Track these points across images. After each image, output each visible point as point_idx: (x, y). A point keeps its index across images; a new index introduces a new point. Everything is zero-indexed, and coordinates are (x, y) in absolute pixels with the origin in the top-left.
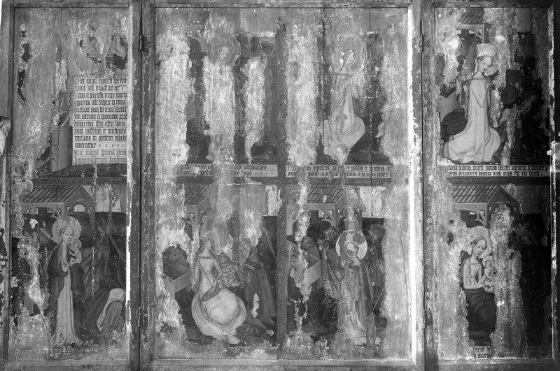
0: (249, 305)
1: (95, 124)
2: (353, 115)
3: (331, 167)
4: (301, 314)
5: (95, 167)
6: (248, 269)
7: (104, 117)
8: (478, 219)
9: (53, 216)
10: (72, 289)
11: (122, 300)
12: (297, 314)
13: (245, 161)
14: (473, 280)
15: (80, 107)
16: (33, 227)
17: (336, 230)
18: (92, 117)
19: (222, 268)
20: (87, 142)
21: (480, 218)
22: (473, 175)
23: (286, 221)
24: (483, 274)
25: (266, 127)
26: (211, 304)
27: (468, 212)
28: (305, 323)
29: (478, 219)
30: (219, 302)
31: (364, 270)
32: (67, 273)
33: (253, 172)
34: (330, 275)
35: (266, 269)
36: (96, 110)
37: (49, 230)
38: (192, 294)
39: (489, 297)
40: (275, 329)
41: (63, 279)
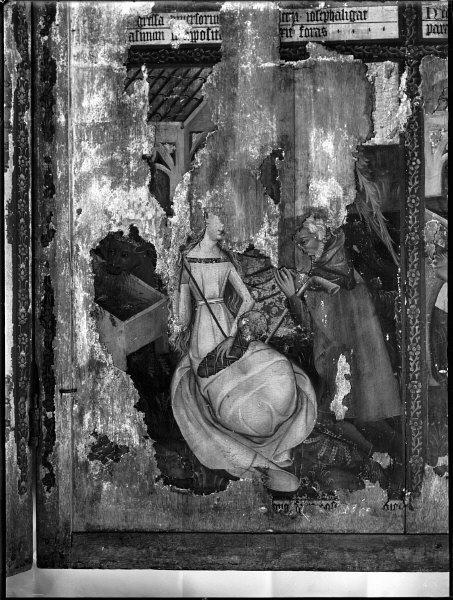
0: (324, 388)
6: (321, 289)
19: (251, 287)
23: (421, 157)
26: (223, 384)
30: (243, 378)
35: (371, 287)
38: (172, 359)
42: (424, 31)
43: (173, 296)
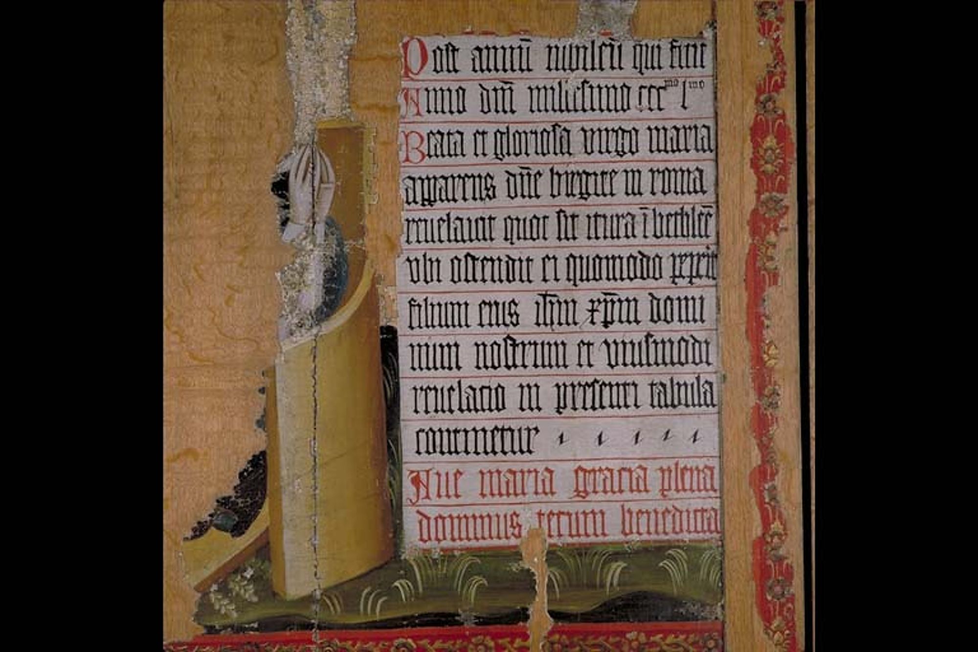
1: (527, 311)
5: (535, 562)
7: (582, 269)
18: (513, 270)
20: (486, 420)
36: (532, 229)
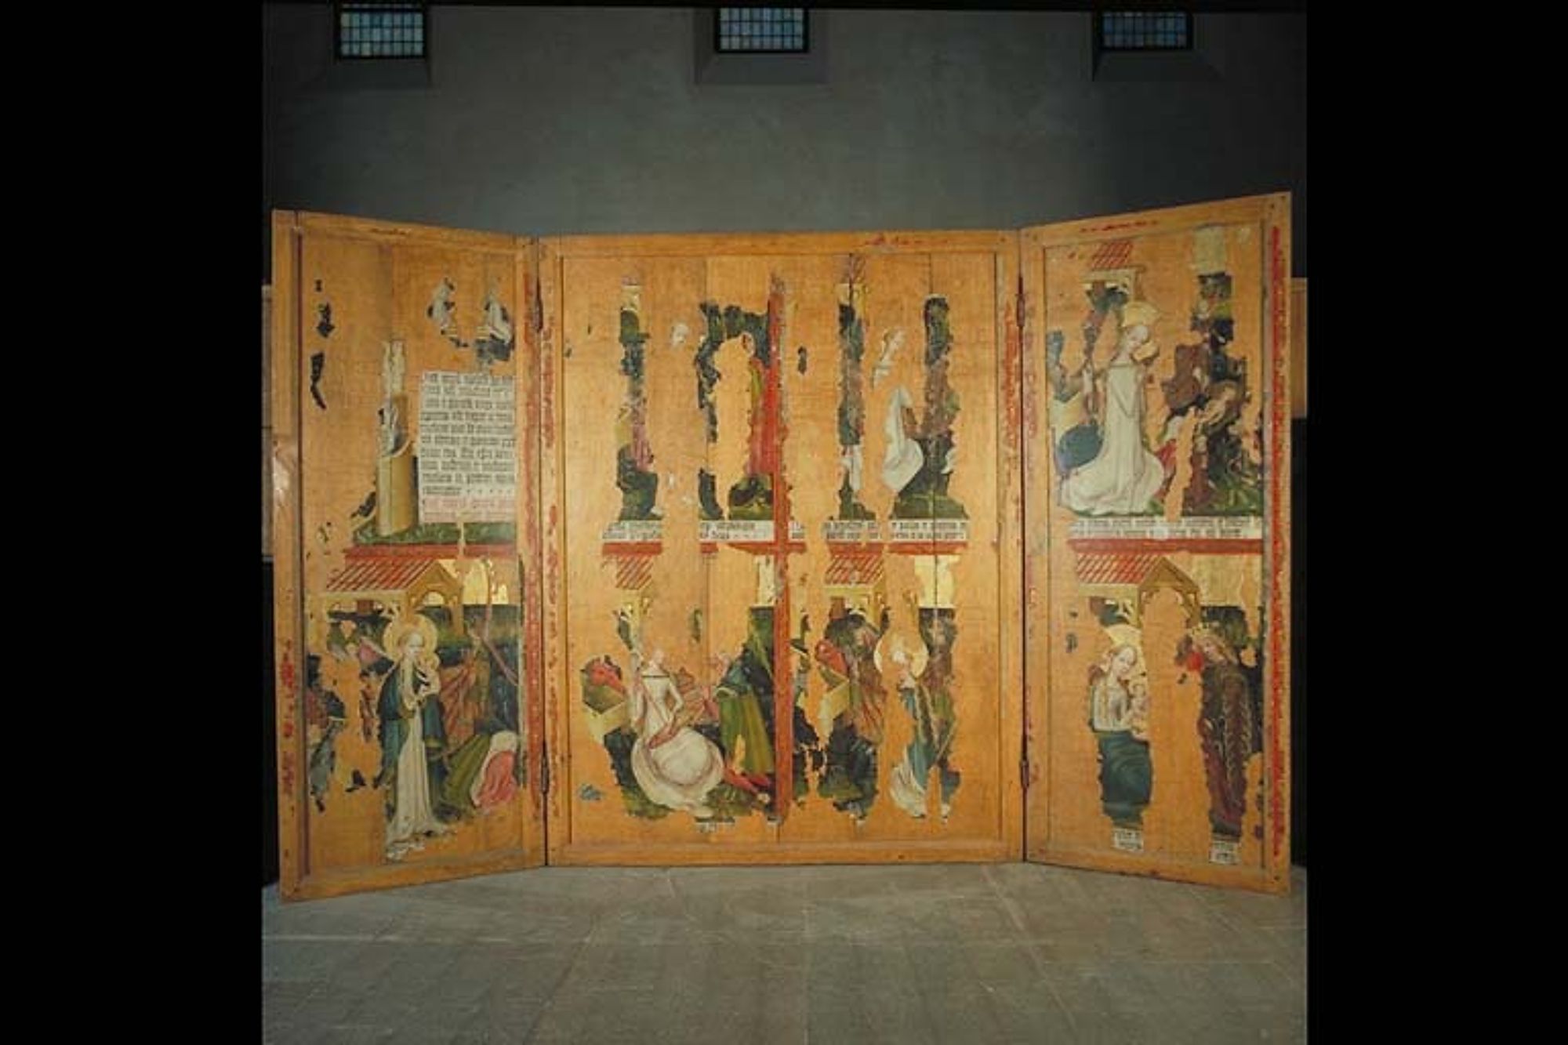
1: (458, 453)
2: (903, 436)
3: (866, 523)
4: (815, 767)
5: (460, 527)
6: (726, 695)
8: (1120, 612)
9: (385, 614)
10: (424, 738)
11: (514, 749)
12: (809, 768)
13: (718, 516)
14: (1111, 717)
15: (431, 422)
16: (347, 636)
17: (874, 630)
18: (453, 441)
19: (682, 693)
20: (446, 485)
21: (1126, 610)
22: (1114, 535)
24: (1129, 707)
25: (753, 458)
26: (664, 753)
27: (1103, 600)
28: (823, 780)
29: (1120, 612)
31: (921, 694)
32: (414, 711)
33: (732, 533)
34: (863, 701)
35: (757, 694)
36: (460, 429)
37: (379, 641)
38: (632, 738)
39: (1139, 748)
40: (771, 792)
41: (406, 721)
42: (790, 535)
43: (632, 699)
